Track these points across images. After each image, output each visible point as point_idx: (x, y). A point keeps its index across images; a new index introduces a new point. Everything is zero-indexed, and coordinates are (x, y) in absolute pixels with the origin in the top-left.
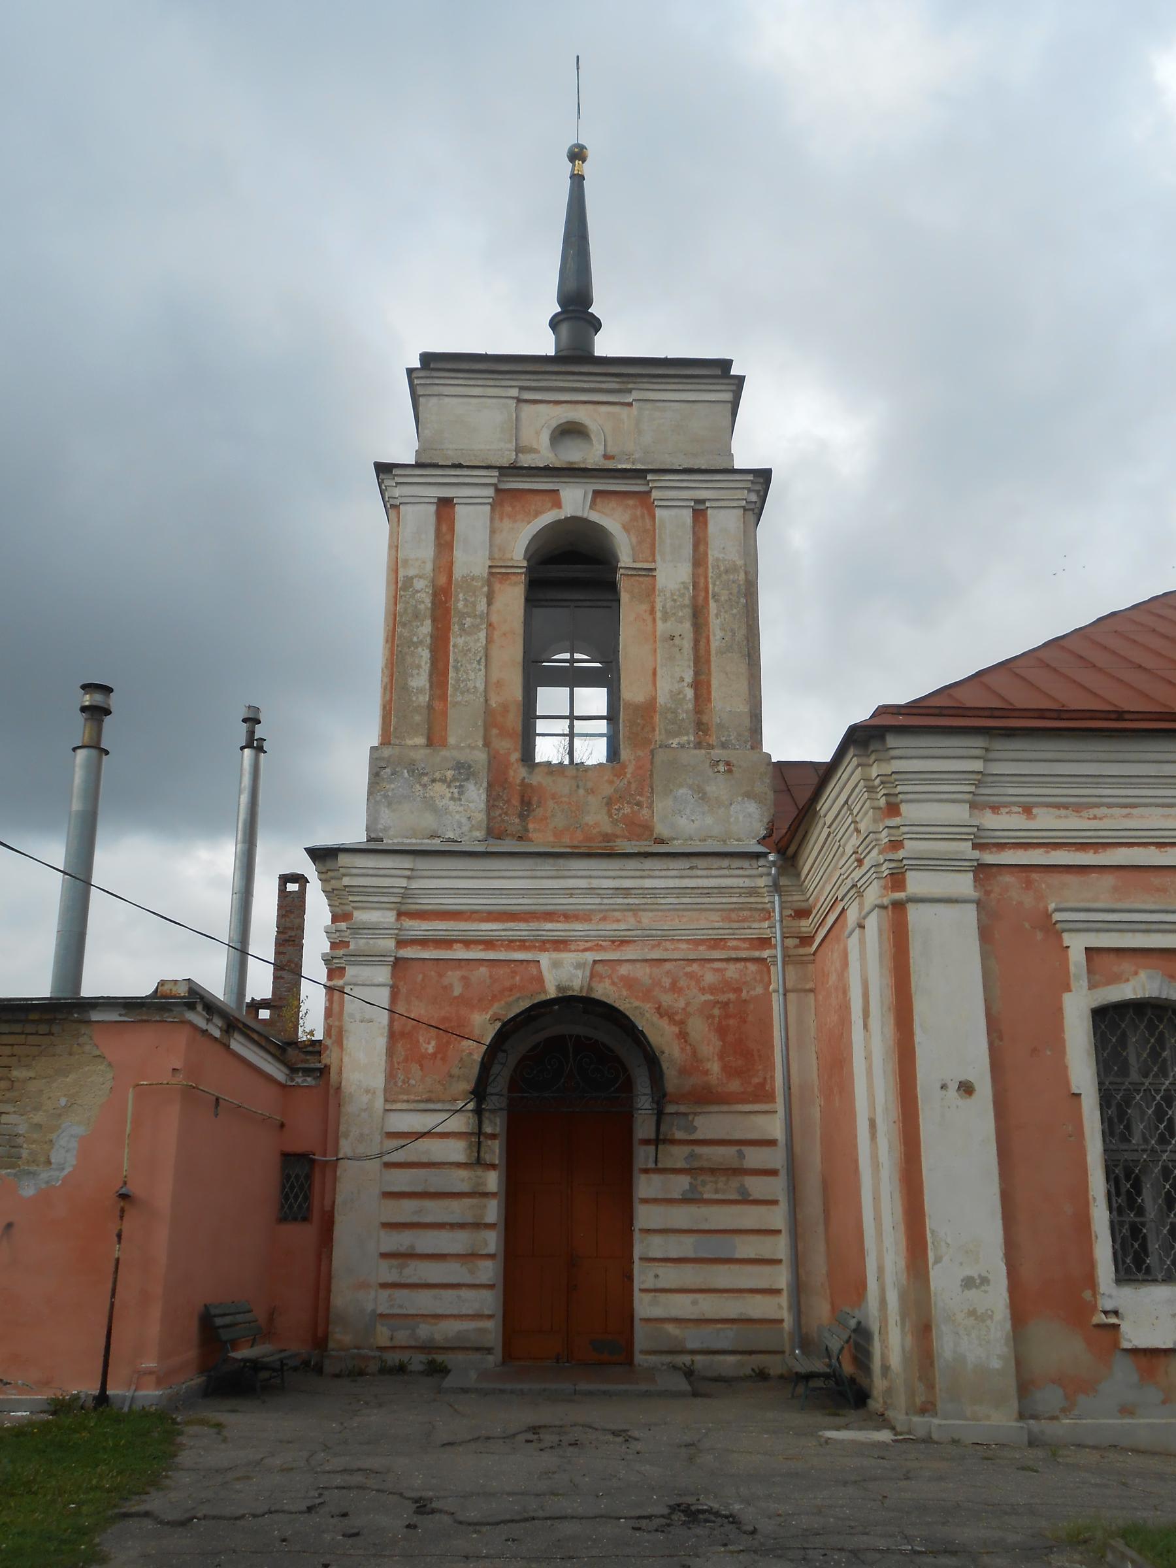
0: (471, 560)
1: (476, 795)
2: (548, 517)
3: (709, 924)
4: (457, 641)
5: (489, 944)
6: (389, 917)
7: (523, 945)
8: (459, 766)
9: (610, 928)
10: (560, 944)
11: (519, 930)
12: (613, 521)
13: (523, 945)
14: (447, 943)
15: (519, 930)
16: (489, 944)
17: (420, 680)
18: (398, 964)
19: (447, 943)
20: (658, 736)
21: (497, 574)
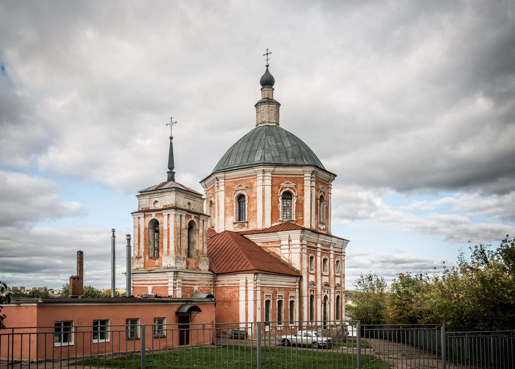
0: (183, 226)
1: (185, 262)
2: (190, 219)
3: (206, 283)
4: (182, 238)
5: (189, 284)
6: (180, 281)
7: (192, 285)
8: (184, 258)
9: (200, 283)
10: (195, 285)
11: (192, 283)
12: (196, 221)
13: (192, 285)
14: (185, 284)
15: (192, 283)
16: (189, 284)
17: (179, 244)
18: (182, 287)
19: (185, 284)
20: (199, 255)
21: (186, 228)
